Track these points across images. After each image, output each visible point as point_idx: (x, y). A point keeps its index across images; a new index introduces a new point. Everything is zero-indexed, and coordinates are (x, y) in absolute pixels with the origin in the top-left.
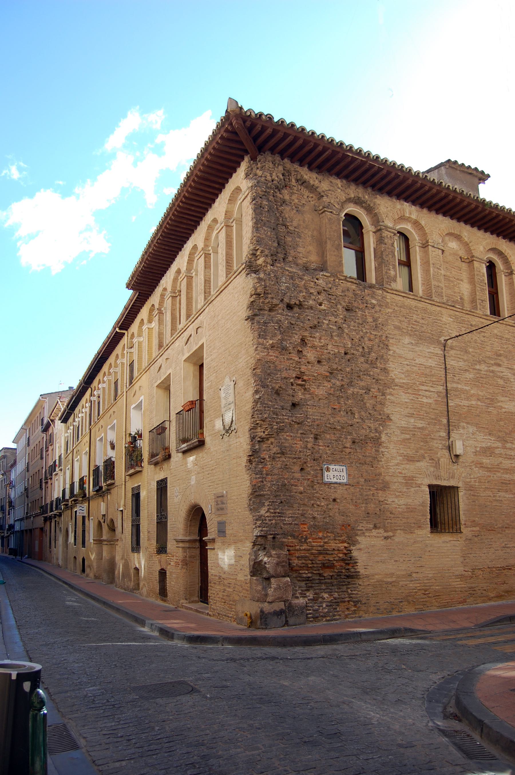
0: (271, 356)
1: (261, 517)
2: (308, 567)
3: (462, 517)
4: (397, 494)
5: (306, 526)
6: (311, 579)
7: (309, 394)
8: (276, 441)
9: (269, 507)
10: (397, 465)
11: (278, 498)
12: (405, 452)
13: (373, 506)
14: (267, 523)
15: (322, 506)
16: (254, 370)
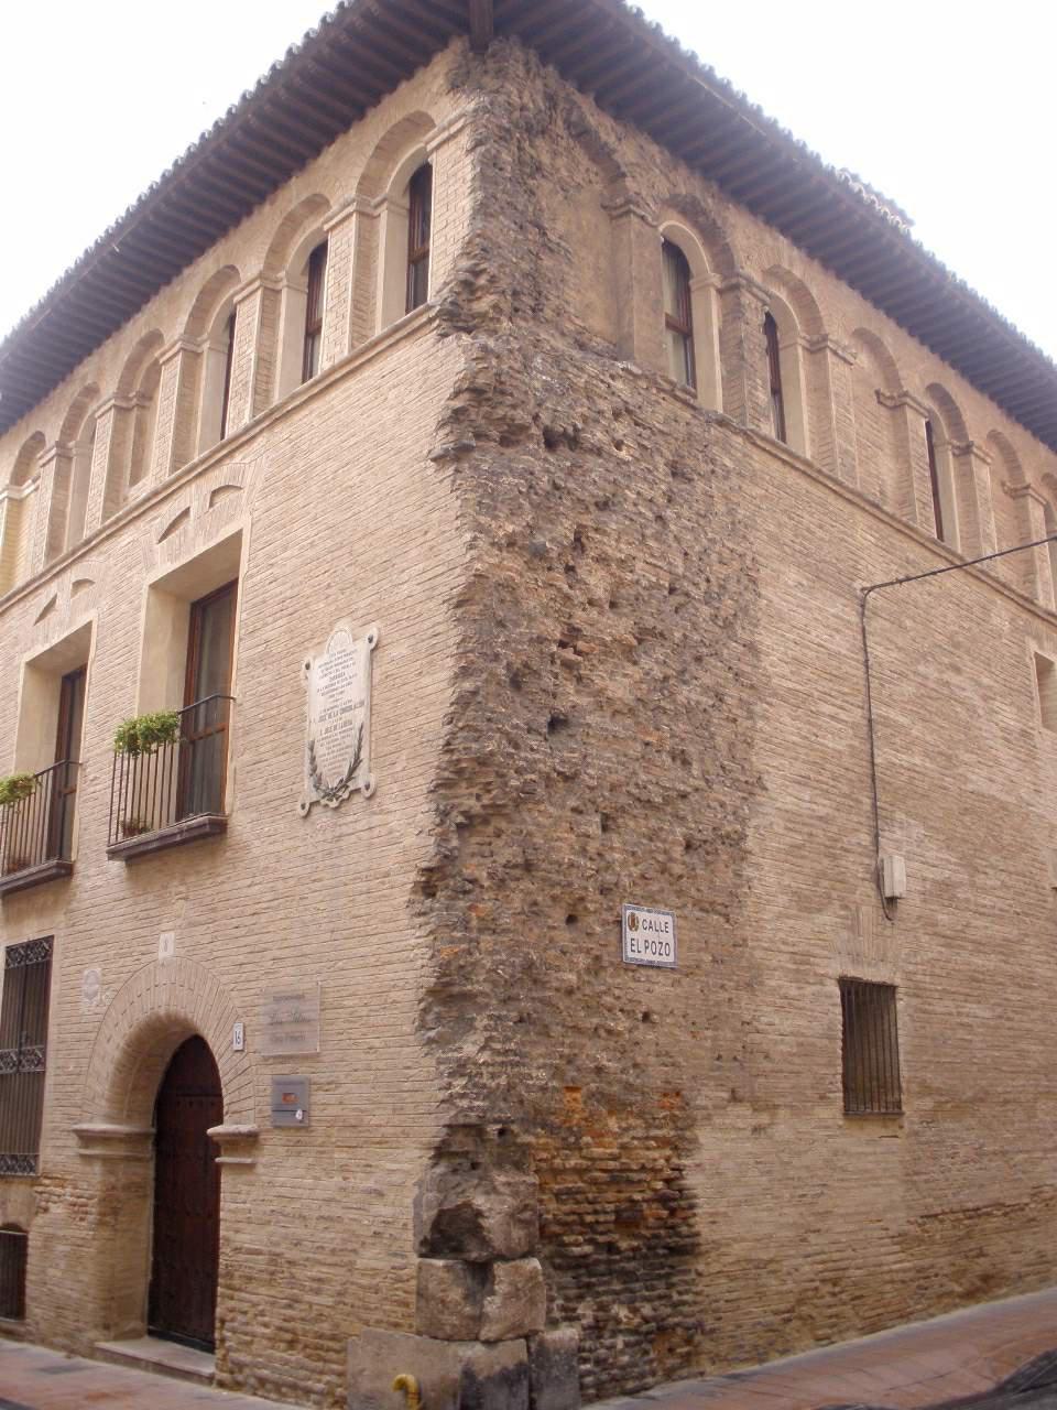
0: (510, 569)
1: (464, 1066)
2: (582, 1223)
3: (905, 1073)
4: (779, 1002)
5: (577, 1095)
6: (590, 1260)
7: (589, 694)
8: (513, 828)
9: (487, 1034)
10: (778, 918)
11: (512, 1005)
12: (793, 884)
13: (730, 1035)
14: (484, 1086)
15: (619, 1034)
16: (459, 605)
